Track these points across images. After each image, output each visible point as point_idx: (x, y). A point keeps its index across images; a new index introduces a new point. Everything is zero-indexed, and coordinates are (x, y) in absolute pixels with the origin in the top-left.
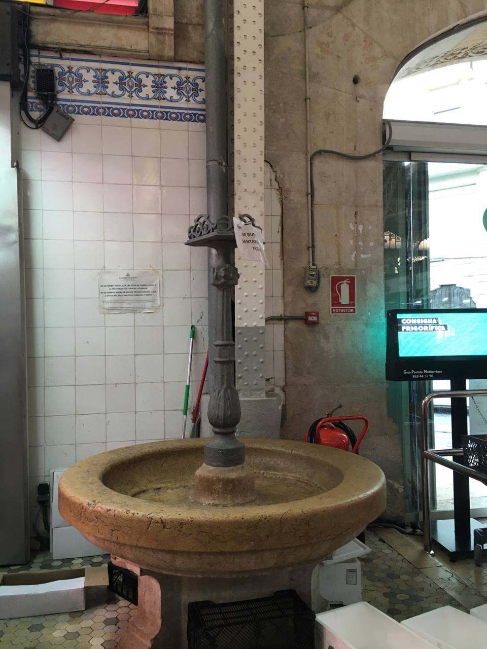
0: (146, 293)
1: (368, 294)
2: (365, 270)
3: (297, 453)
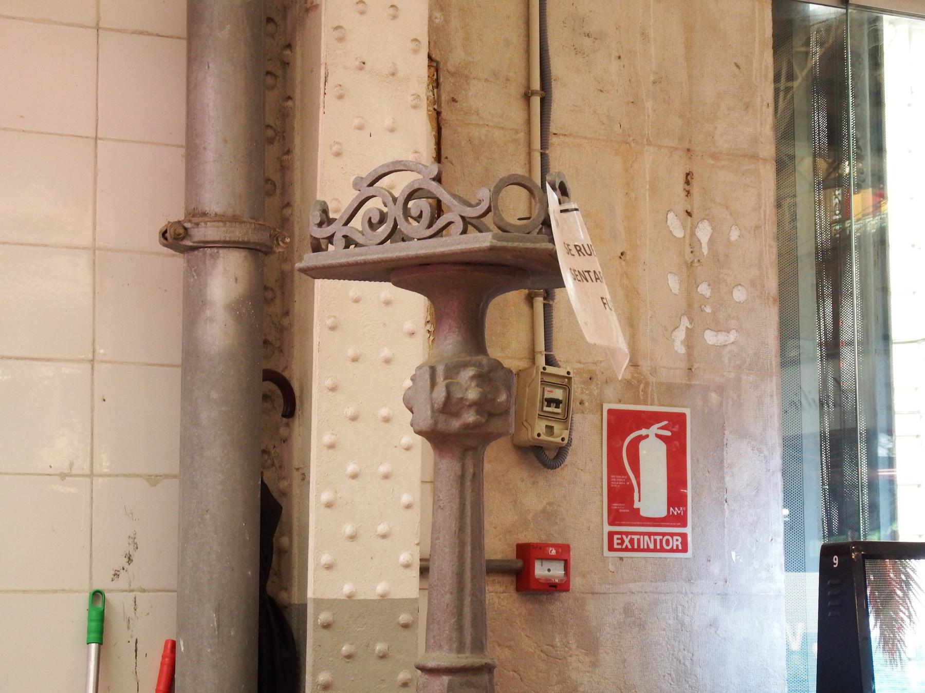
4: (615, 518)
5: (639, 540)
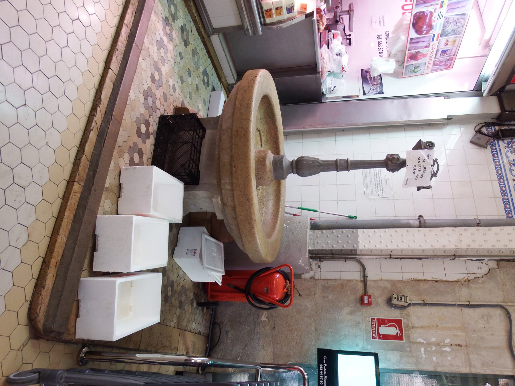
0: (377, 190)
1: (390, 352)
2: (410, 351)
4: (378, 320)
5: (374, 326)
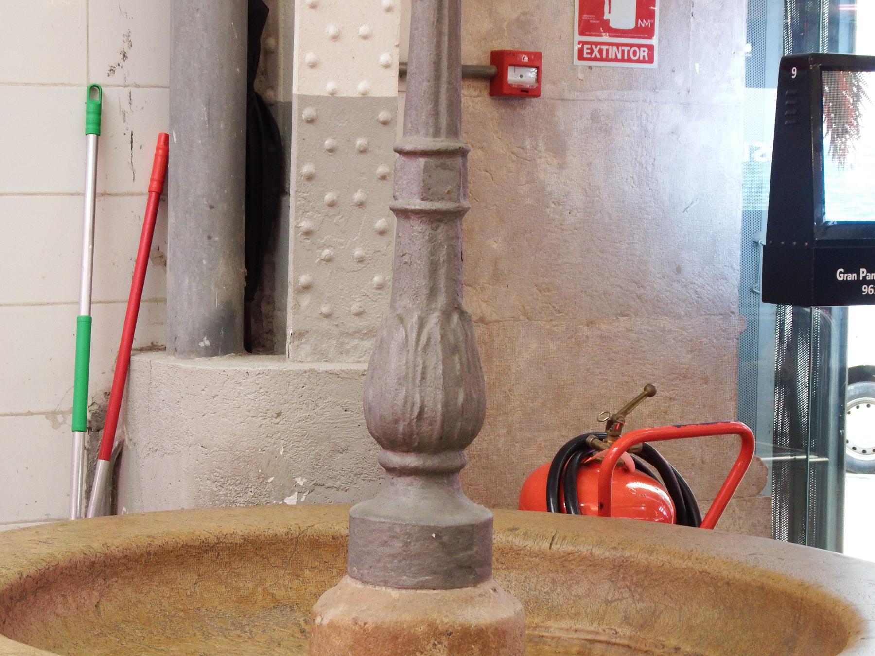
3: (570, 548)
4: (586, 29)
5: (607, 50)
